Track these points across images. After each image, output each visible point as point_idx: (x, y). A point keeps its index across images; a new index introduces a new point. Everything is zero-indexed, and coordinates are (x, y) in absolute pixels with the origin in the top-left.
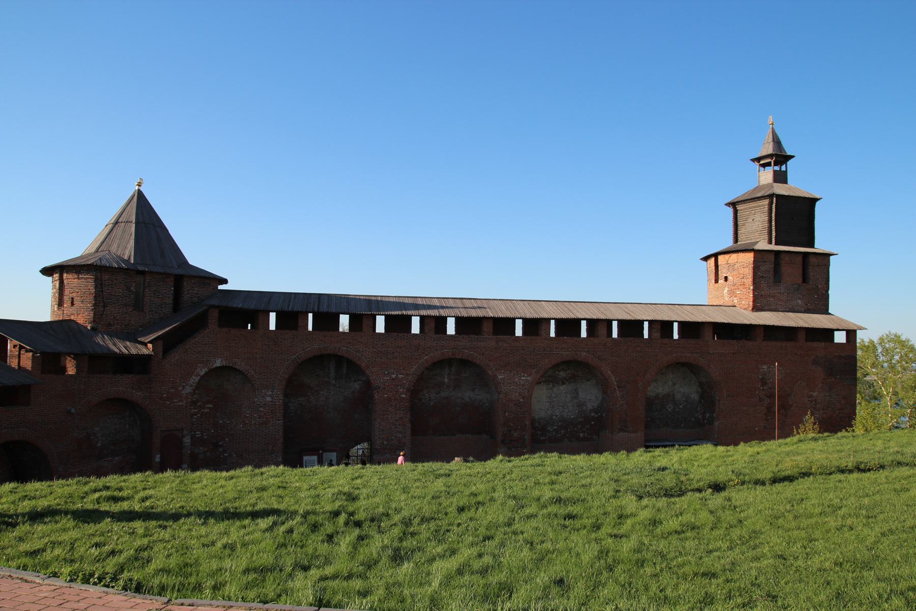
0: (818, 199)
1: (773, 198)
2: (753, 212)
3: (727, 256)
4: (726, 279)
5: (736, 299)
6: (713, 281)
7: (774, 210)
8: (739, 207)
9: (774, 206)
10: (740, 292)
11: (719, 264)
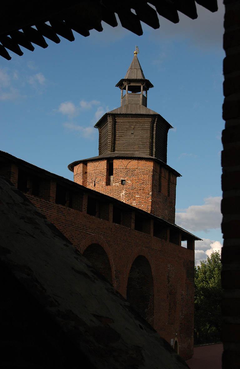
1: (156, 118)
2: (133, 127)
3: (125, 162)
5: (135, 202)
6: (104, 183)
8: (118, 120)
10: (139, 196)
11: (114, 167)
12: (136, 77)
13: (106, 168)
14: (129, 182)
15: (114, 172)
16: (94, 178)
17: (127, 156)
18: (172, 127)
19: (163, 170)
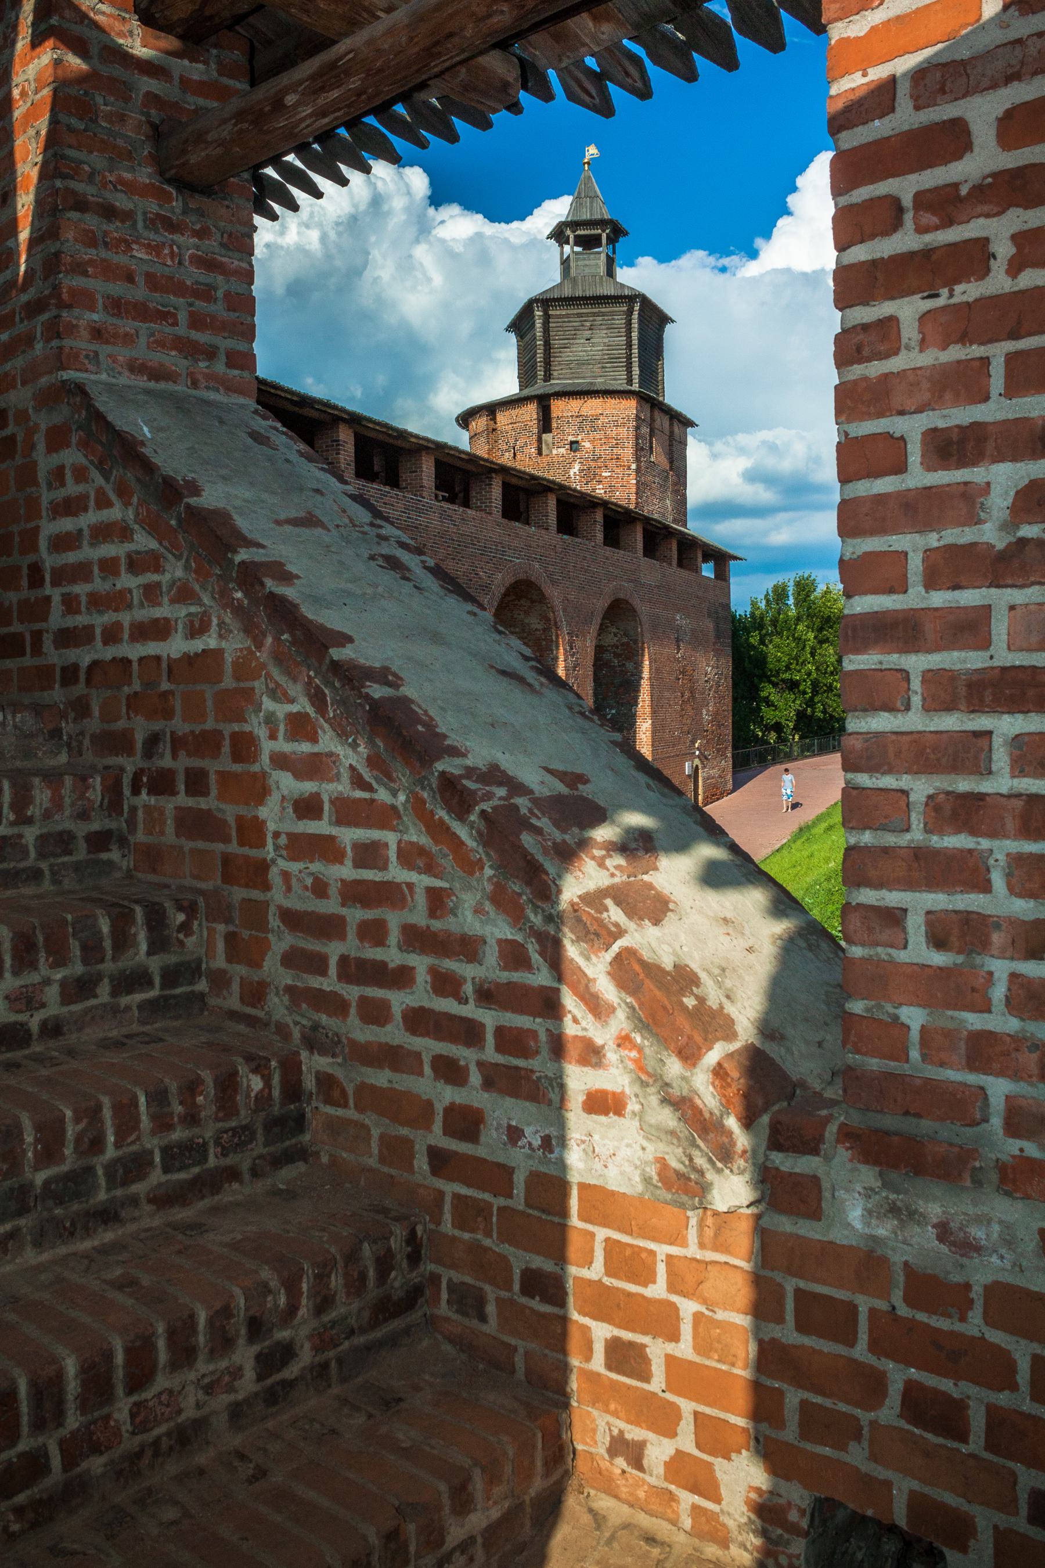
0: (673, 321)
2: (588, 324)
4: (574, 446)
5: (601, 486)
7: (635, 325)
9: (635, 316)
11: (554, 415)
12: (591, 214)
13: (535, 417)
14: (587, 445)
15: (554, 425)
16: (512, 441)
17: (579, 389)
18: (673, 321)
19: (657, 415)
